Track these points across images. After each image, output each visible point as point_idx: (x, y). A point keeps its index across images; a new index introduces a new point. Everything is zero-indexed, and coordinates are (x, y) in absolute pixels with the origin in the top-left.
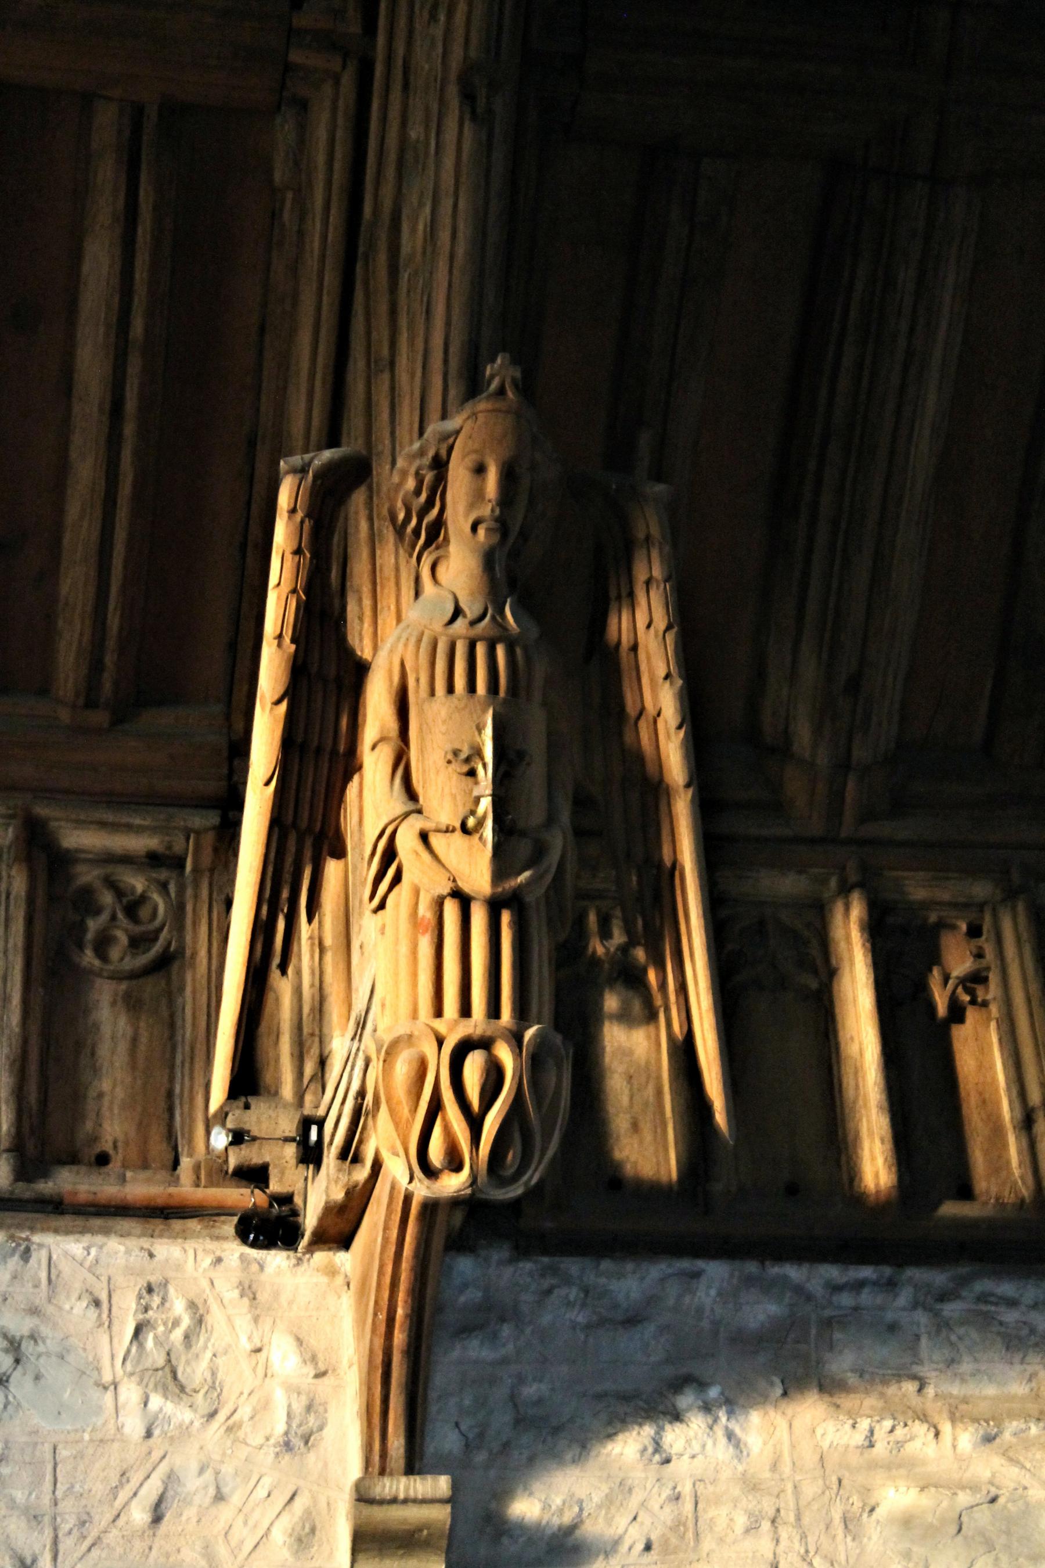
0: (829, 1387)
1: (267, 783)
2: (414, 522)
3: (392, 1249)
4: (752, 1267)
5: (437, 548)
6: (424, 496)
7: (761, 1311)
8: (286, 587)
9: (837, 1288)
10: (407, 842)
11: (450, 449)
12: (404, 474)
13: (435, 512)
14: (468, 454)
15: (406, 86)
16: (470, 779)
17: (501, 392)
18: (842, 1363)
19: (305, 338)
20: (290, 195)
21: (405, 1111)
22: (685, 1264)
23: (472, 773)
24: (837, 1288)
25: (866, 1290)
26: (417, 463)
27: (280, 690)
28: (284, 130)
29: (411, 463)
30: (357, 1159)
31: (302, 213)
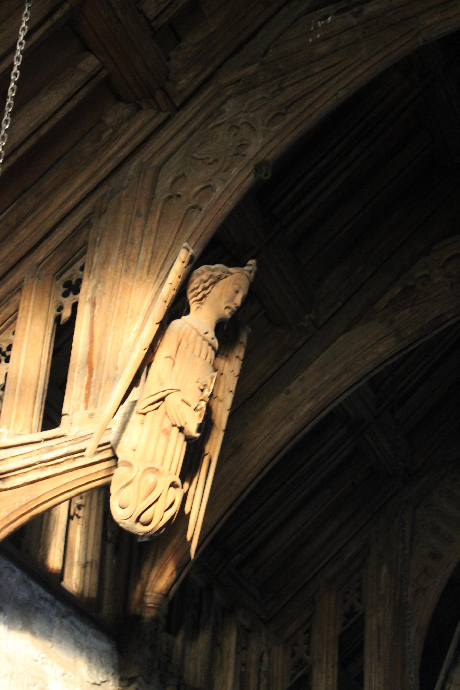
0: (33, 633)
1: (145, 349)
2: (199, 290)
4: (25, 577)
5: (200, 303)
6: (207, 284)
7: (24, 594)
9: (41, 598)
11: (226, 277)
12: (203, 273)
13: (206, 292)
14: (237, 284)
15: (190, 136)
16: (200, 392)
17: (251, 272)
18: (36, 626)
19: (82, 177)
20: (111, 131)
21: (142, 494)
22: (11, 565)
23: (202, 390)
24: (41, 598)
25: (48, 603)
27: (159, 320)
28: (123, 110)
29: (207, 271)
31: (111, 140)
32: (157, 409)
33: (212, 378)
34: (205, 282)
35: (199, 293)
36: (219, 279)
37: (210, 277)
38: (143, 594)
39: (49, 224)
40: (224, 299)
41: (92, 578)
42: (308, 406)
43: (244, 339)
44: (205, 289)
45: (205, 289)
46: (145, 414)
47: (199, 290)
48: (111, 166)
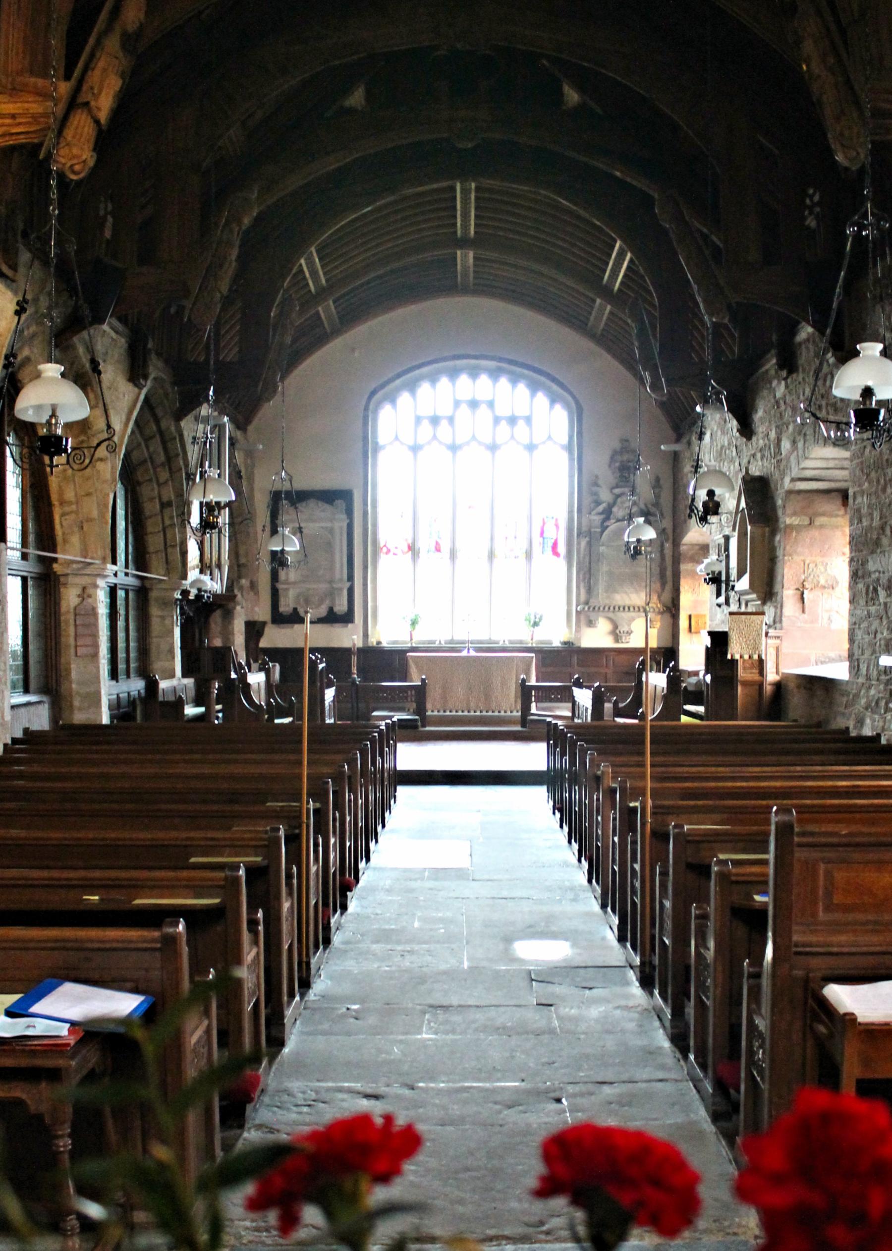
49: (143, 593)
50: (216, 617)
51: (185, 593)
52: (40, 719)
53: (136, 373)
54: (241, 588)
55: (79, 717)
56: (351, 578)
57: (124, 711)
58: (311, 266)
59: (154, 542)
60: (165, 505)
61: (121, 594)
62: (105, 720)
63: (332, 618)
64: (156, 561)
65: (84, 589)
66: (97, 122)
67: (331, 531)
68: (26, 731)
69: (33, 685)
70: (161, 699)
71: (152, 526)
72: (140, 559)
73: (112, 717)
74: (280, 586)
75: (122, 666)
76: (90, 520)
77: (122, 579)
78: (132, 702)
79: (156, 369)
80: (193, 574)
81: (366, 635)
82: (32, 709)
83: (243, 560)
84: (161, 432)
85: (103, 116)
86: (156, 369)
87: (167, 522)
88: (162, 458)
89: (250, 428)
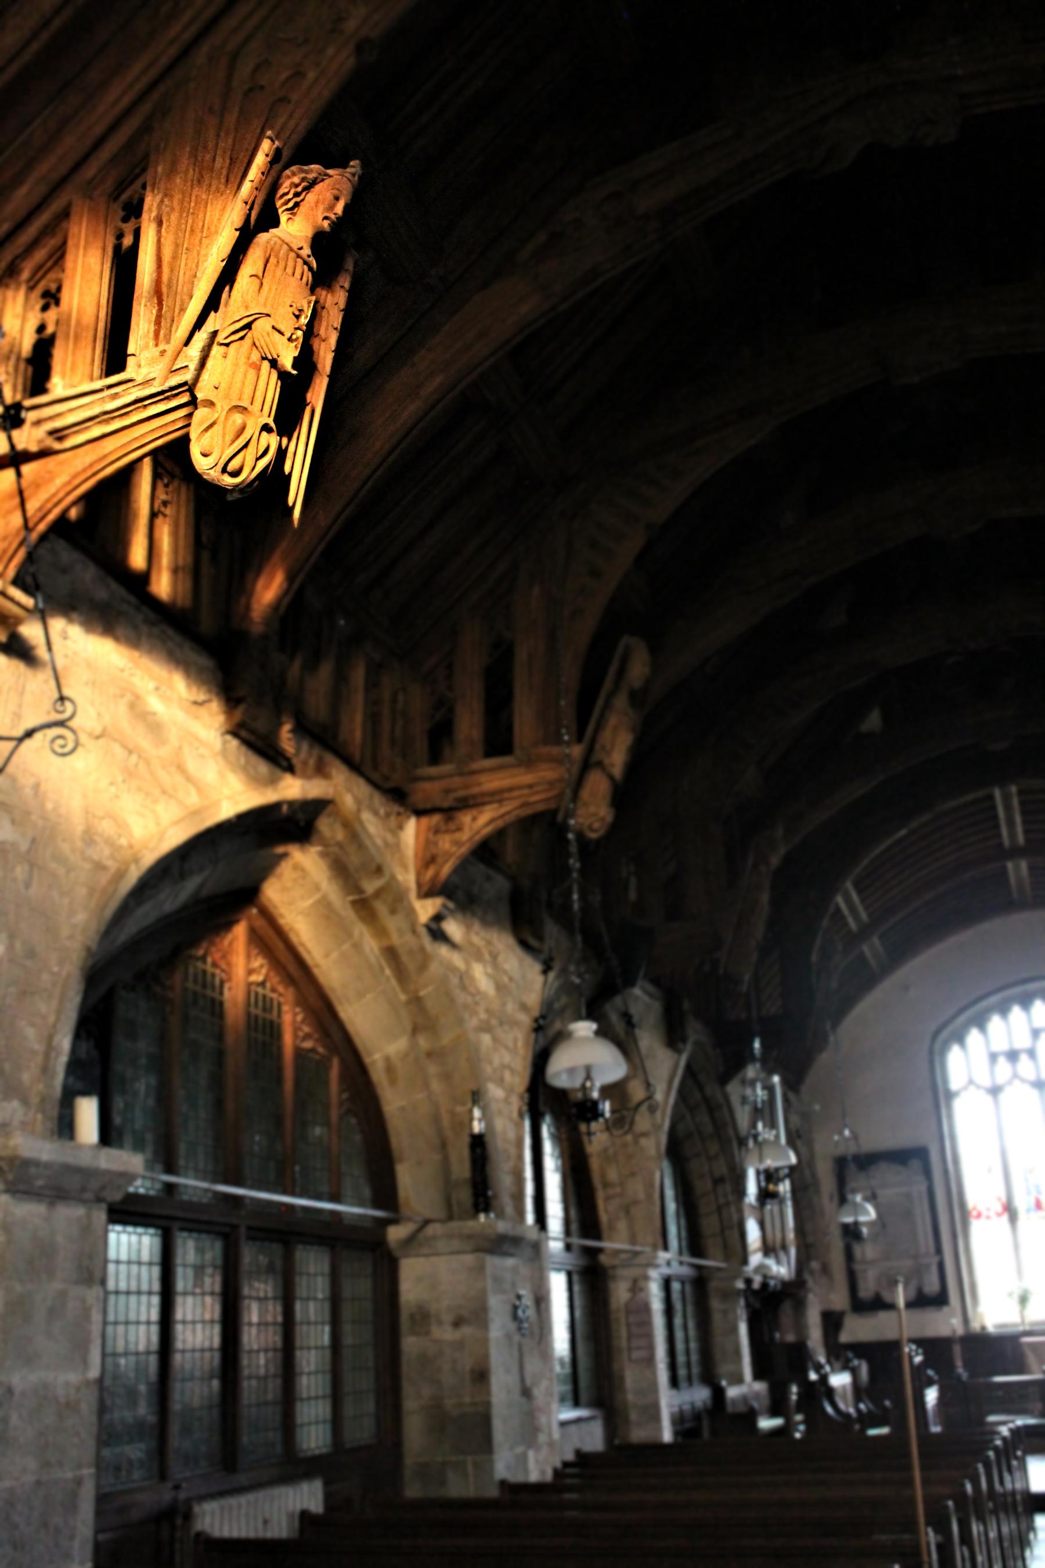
0: (117, 639)
2: (290, 196)
3: (69, 488)
6: (299, 189)
8: (255, 184)
10: (262, 326)
11: (323, 180)
12: (294, 174)
13: (298, 199)
17: (354, 175)
18: (120, 631)
19: (137, 67)
23: (298, 317)
26: (303, 175)
30: (60, 439)
32: (242, 338)
33: (309, 303)
34: (297, 186)
35: (290, 200)
36: (313, 183)
37: (303, 179)
38: (248, 608)
39: (99, 130)
40: (321, 207)
41: (186, 585)
42: (438, 380)
43: (350, 265)
44: (297, 195)
45: (297, 195)
46: (227, 345)
47: (290, 196)
48: (173, 51)
49: (700, 1284)
50: (786, 1311)
51: (749, 1281)
52: (594, 1439)
53: (673, 1038)
54: (812, 1273)
55: (638, 1435)
56: (939, 1250)
57: (688, 1425)
58: (848, 902)
59: (709, 1224)
60: (718, 1181)
61: (676, 1286)
62: (667, 1436)
63: (921, 1301)
64: (712, 1245)
65: (635, 1281)
66: (611, 778)
67: (908, 1196)
68: (579, 1453)
69: (584, 1396)
70: (730, 1409)
71: (705, 1207)
72: (695, 1245)
73: (676, 1433)
74: (857, 1267)
75: (682, 1372)
76: (636, 1202)
77: (676, 1269)
78: (697, 1416)
79: (695, 1031)
80: (756, 1259)
81: (966, 1320)
82: (583, 1425)
83: (810, 1239)
84: (706, 1100)
85: (617, 771)
86: (695, 1031)
87: (722, 1201)
88: (709, 1128)
89: (804, 1089)
